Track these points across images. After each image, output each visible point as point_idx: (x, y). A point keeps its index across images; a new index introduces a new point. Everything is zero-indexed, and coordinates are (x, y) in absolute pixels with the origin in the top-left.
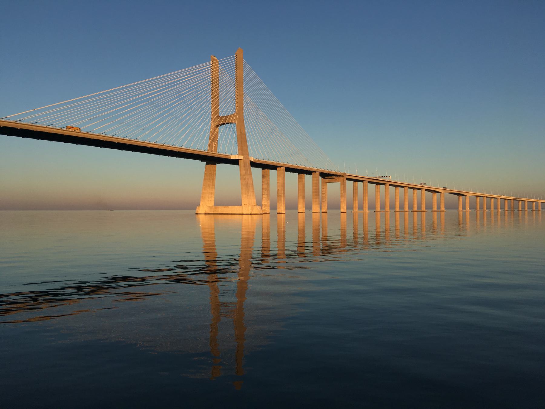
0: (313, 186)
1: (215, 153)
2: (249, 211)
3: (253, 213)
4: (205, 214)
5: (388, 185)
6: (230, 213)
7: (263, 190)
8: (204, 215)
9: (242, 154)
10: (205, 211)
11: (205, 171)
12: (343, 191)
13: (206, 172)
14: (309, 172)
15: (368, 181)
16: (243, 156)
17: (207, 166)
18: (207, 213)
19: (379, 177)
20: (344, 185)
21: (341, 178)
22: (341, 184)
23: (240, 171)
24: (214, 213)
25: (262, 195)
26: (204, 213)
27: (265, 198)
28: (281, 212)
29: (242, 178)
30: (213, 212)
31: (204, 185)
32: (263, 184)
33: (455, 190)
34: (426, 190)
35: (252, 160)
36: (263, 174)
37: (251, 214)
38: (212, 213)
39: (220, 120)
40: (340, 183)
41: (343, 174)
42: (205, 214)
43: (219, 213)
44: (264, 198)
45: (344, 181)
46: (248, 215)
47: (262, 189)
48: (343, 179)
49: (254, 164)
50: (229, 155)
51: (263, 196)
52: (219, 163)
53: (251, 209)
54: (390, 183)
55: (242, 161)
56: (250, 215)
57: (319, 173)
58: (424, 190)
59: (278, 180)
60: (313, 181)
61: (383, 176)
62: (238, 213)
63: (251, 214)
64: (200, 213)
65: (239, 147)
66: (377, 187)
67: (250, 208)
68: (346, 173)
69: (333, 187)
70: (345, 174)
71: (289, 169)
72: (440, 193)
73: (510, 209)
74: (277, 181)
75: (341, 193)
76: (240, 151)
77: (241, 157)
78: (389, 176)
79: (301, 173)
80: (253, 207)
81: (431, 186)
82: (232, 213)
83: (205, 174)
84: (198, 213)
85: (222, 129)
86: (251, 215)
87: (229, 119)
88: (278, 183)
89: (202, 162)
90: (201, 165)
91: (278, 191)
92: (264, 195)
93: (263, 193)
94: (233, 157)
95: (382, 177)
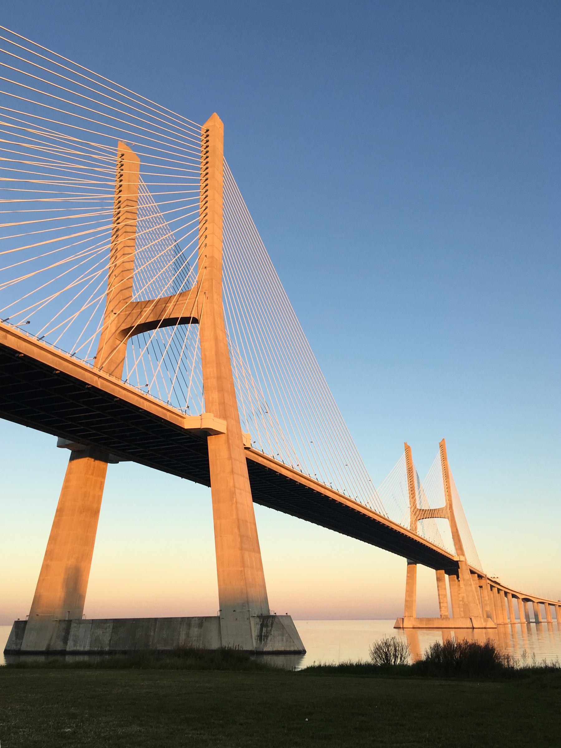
2: (482, 624)
3: (487, 627)
4: (414, 628)
6: (453, 627)
7: (440, 597)
8: (412, 629)
11: (408, 573)
12: (487, 597)
13: (409, 575)
16: (464, 557)
17: (409, 565)
18: (416, 627)
25: (440, 603)
26: (412, 627)
27: (443, 606)
31: (407, 591)
32: (439, 588)
36: (438, 576)
37: (485, 628)
41: (485, 576)
42: (414, 628)
44: (443, 606)
46: (482, 629)
47: (439, 595)
48: (485, 582)
51: (441, 604)
55: (464, 562)
57: (476, 575)
61: (493, 578)
62: (466, 627)
63: (485, 628)
65: (457, 547)
66: (481, 590)
72: (516, 599)
73: (545, 619)
76: (459, 552)
79: (452, 575)
80: (486, 621)
82: (456, 627)
83: (408, 577)
84: (401, 627)
86: (485, 629)
92: (443, 603)
93: (442, 601)
94: (455, 559)
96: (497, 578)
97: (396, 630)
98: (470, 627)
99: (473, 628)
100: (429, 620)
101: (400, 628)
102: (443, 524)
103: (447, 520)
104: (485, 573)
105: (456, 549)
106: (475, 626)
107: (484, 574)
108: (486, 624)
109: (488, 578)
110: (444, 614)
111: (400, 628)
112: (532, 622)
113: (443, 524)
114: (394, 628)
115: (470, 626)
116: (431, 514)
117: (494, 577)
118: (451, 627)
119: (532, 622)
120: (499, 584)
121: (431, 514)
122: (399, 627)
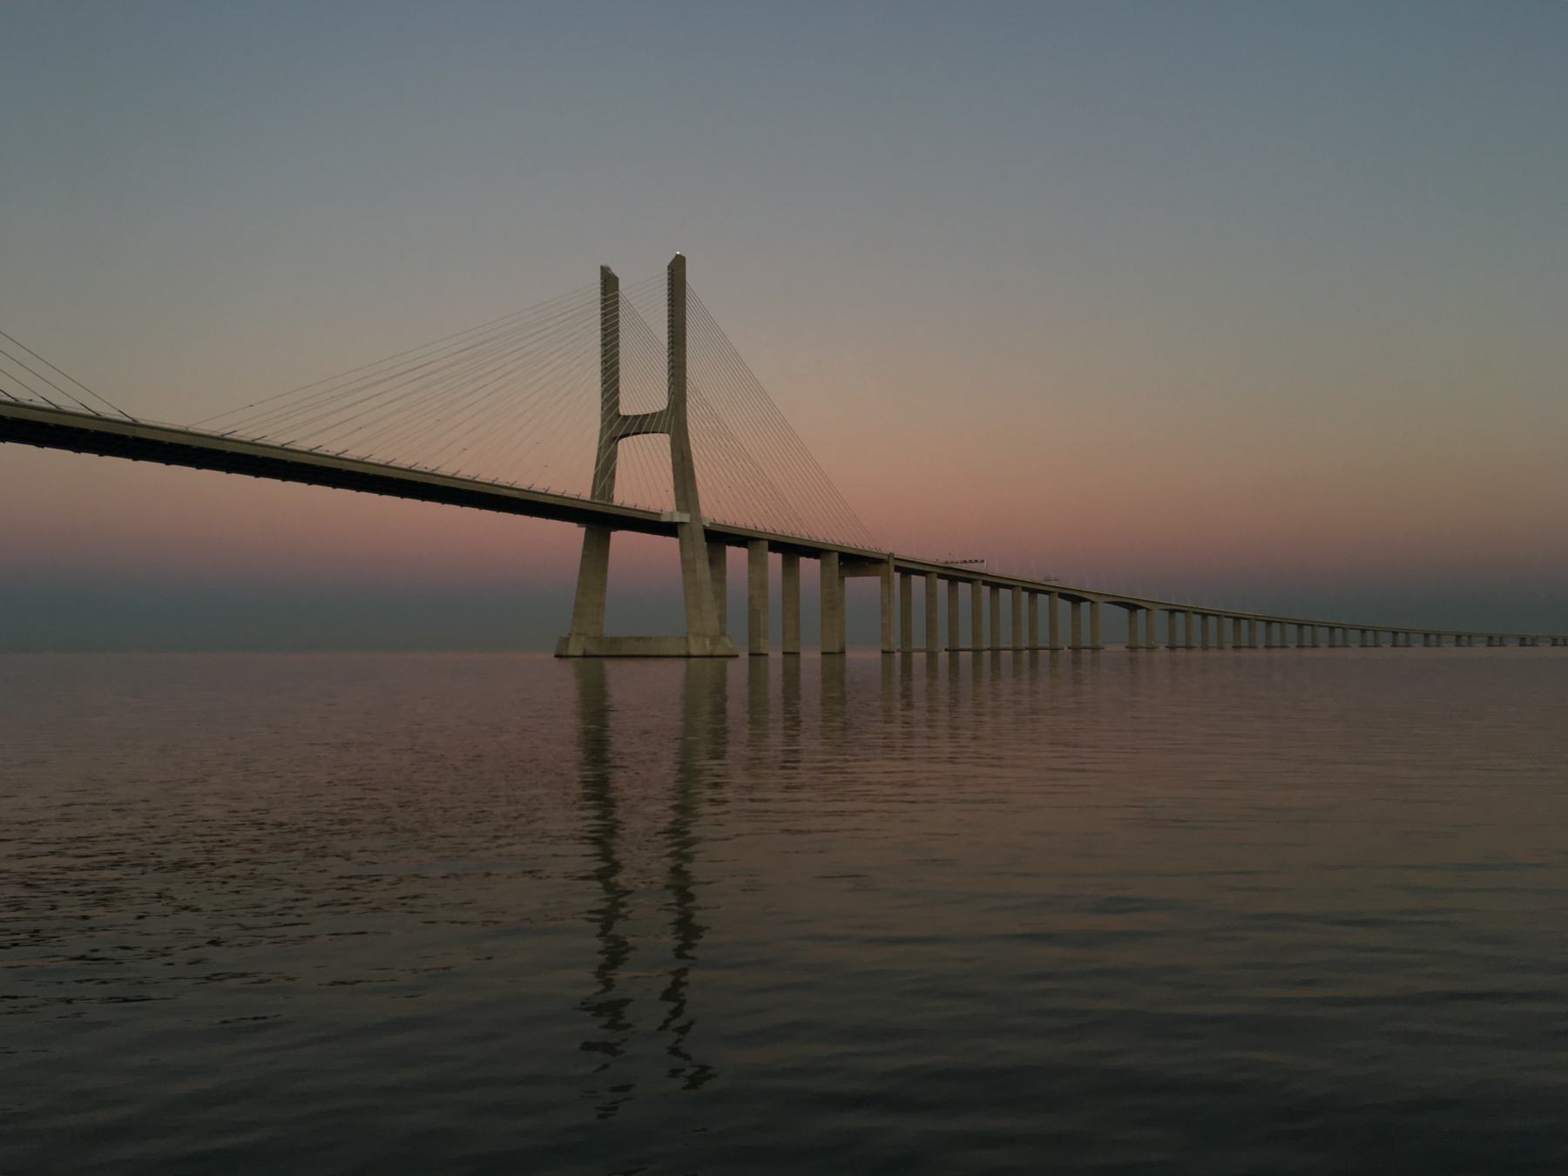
0: (822, 586)
1: (609, 503)
3: (716, 653)
4: (584, 656)
5: (980, 582)
6: (655, 653)
8: (579, 659)
9: (687, 510)
10: (584, 652)
14: (814, 551)
15: (938, 574)
16: (688, 515)
18: (588, 654)
19: (952, 563)
20: (887, 582)
21: (884, 566)
22: (882, 582)
23: (681, 550)
26: (580, 653)
28: (757, 652)
29: (687, 565)
33: (1124, 593)
34: (1062, 596)
35: (708, 525)
38: (605, 653)
39: (620, 426)
40: (877, 579)
41: (886, 557)
42: (584, 656)
43: (623, 653)
45: (889, 572)
49: (719, 538)
50: (659, 512)
52: (615, 531)
53: (711, 644)
54: (985, 578)
56: (708, 660)
57: (837, 554)
58: (1056, 595)
59: (750, 571)
60: (823, 572)
62: (676, 653)
67: (708, 642)
68: (893, 554)
69: (862, 587)
70: (890, 555)
71: (776, 545)
72: (1089, 603)
74: (749, 573)
75: (882, 604)
77: (686, 518)
78: (983, 561)
80: (715, 641)
81: (1071, 584)
84: (564, 654)
85: (623, 443)
87: (650, 423)
88: (749, 578)
89: (579, 526)
90: (574, 533)
91: (751, 598)
94: (664, 519)
95: (965, 561)
96: (983, 561)
97: (556, 659)
99: (688, 656)
100: (614, 641)
102: (658, 446)
103: (667, 435)
104: (886, 550)
105: (677, 499)
107: (884, 554)
109: (896, 559)
112: (1141, 648)
113: (658, 446)
114: (556, 656)
115: (683, 652)
116: (640, 425)
117: (957, 563)
118: (650, 653)
119: (1141, 648)
120: (986, 575)
121: (640, 425)
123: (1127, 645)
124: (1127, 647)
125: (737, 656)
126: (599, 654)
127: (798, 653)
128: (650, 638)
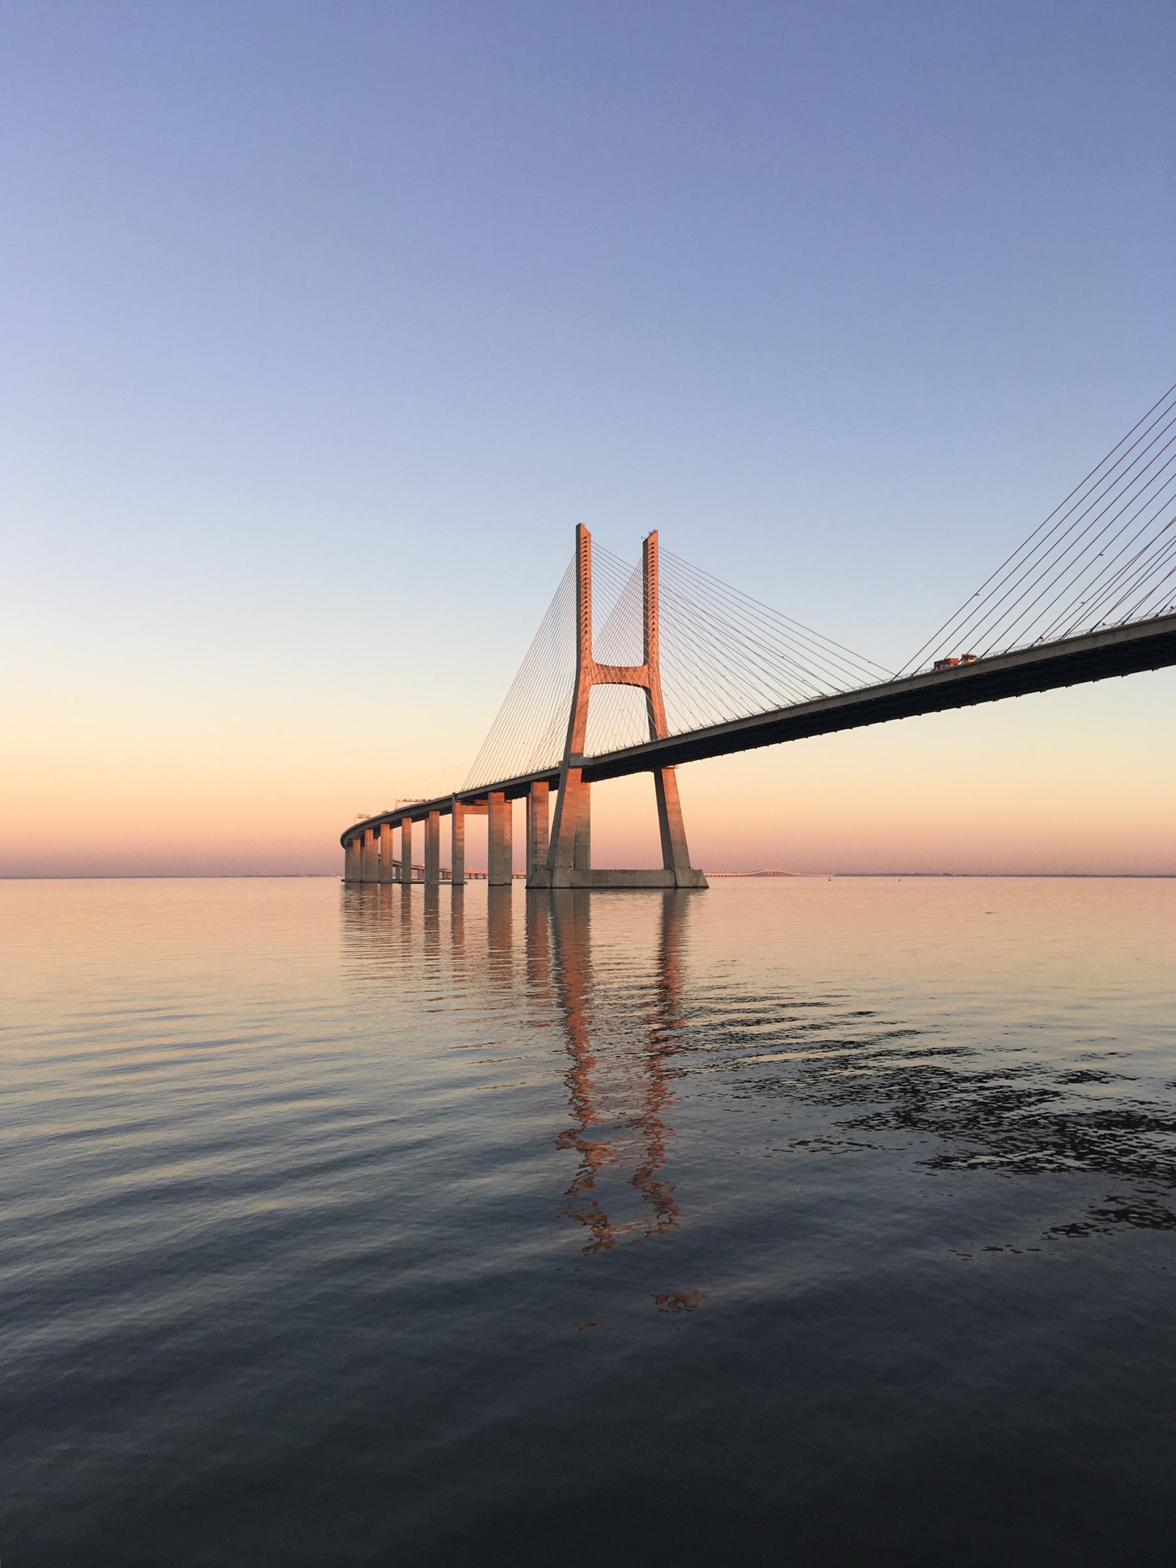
3: (699, 885)
4: (571, 888)
6: (642, 885)
10: (571, 883)
18: (574, 885)
24: (595, 885)
26: (569, 886)
27: (541, 850)
30: (594, 883)
42: (571, 888)
43: (610, 885)
62: (664, 885)
64: (553, 886)
82: (648, 885)
84: (549, 886)
92: (541, 843)
98: (671, 885)
99: (677, 887)
101: (546, 888)
106: (680, 883)
108: (698, 881)
110: (541, 863)
111: (546, 888)
118: (638, 885)
122: (543, 885)
123: (344, 878)
124: (342, 881)
125: (707, 887)
126: (585, 885)
127: (511, 884)
128: (635, 871)
